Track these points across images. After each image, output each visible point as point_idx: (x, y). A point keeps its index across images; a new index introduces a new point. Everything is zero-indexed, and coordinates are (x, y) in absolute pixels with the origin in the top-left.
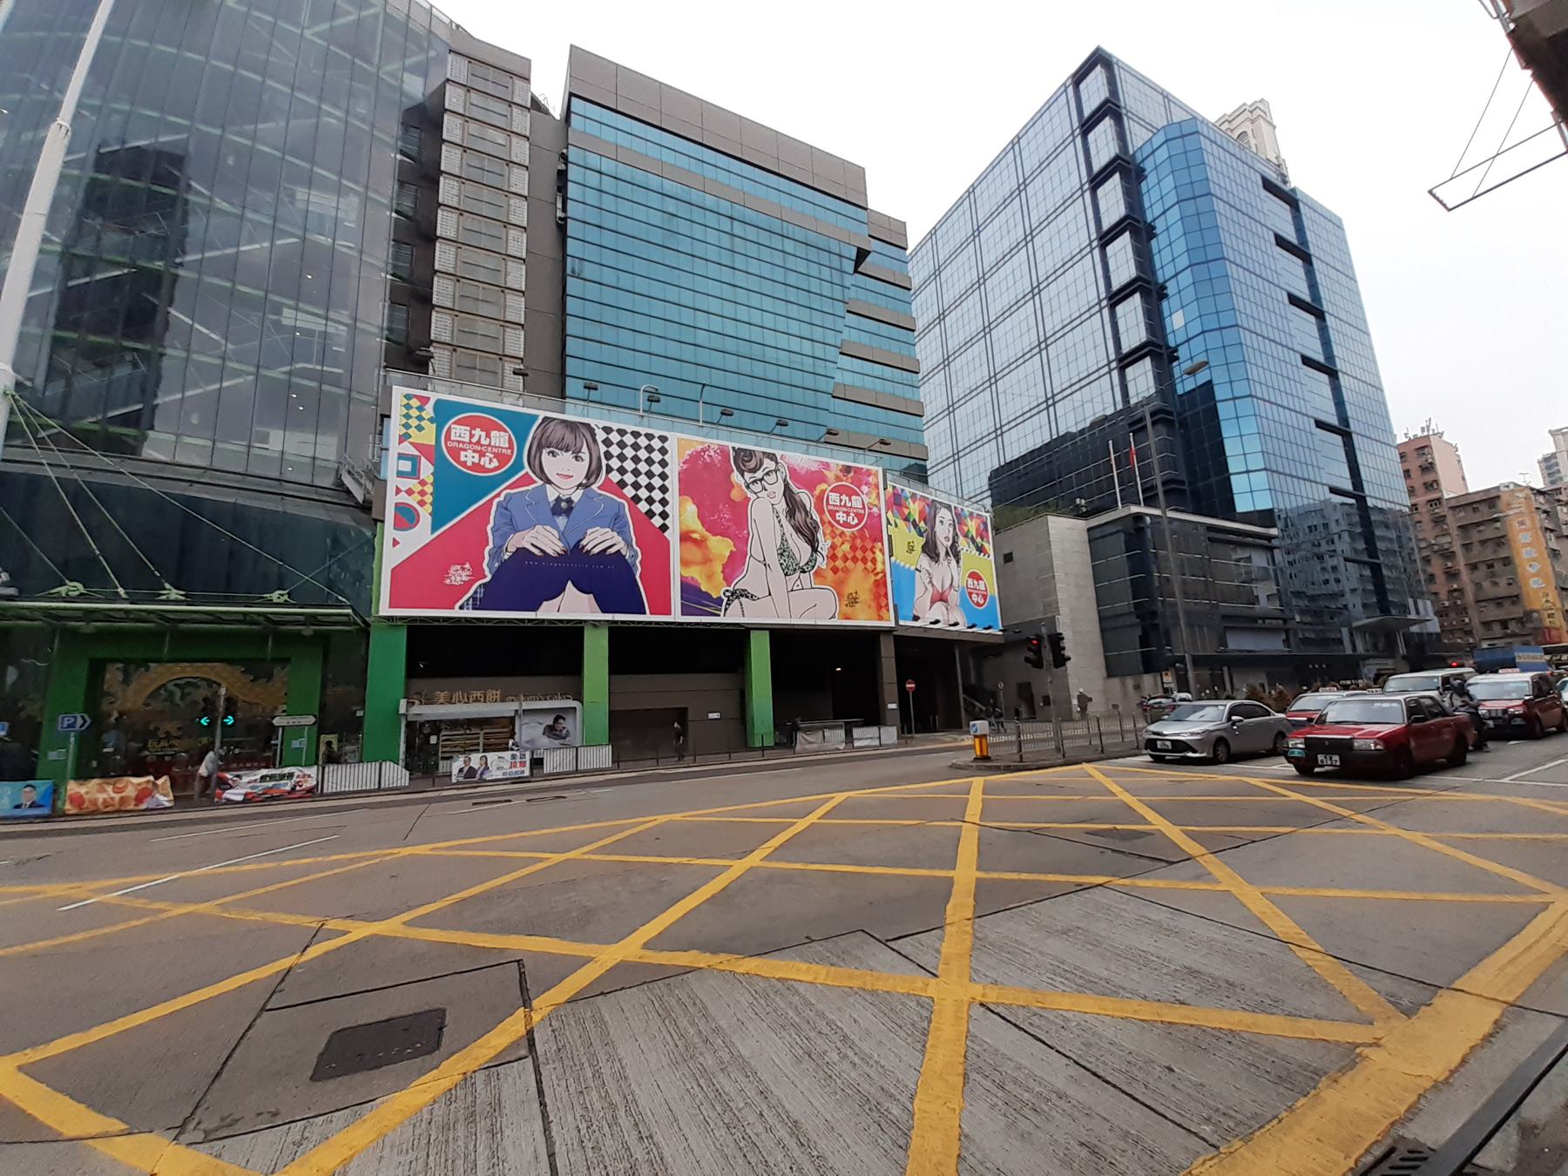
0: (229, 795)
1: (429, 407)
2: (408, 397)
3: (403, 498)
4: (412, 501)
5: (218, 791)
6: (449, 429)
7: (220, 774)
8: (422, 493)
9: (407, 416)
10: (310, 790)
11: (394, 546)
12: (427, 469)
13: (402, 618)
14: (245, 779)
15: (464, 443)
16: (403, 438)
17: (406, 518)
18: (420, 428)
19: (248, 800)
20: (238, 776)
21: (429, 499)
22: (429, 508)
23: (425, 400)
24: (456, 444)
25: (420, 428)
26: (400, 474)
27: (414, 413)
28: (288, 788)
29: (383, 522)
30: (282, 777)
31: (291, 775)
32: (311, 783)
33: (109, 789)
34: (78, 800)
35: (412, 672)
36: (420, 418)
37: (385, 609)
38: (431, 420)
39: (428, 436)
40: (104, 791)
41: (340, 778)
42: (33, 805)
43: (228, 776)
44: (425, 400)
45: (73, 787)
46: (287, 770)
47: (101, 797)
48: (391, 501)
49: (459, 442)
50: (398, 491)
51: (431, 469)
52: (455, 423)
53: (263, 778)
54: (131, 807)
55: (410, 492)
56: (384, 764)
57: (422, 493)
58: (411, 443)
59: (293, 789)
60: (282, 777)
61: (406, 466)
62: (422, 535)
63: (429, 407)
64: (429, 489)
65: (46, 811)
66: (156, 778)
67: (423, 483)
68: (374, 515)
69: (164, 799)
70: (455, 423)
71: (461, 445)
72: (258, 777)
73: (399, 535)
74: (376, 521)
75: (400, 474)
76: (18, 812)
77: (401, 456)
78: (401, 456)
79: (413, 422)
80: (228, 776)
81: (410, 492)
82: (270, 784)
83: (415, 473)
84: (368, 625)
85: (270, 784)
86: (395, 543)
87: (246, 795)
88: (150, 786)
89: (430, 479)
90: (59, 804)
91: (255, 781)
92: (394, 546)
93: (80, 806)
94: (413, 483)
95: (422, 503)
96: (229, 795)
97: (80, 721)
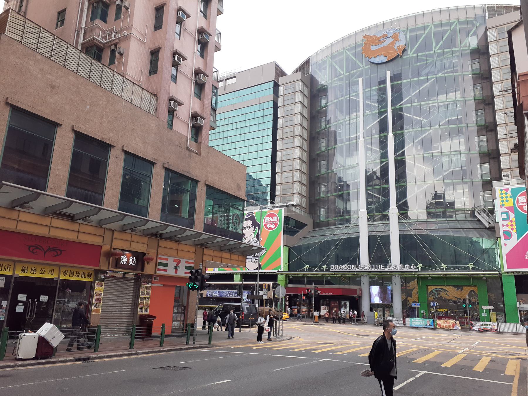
0: (474, 328)
1: (509, 192)
2: (501, 190)
3: (505, 228)
4: (509, 229)
5: (471, 327)
6: (518, 198)
7: (471, 322)
8: (512, 225)
9: (502, 198)
10: (496, 330)
11: (505, 246)
12: (512, 216)
13: (512, 272)
14: (478, 324)
15: (524, 203)
16: (502, 206)
17: (508, 236)
18: (507, 201)
19: (480, 331)
20: (475, 323)
21: (514, 227)
22: (515, 231)
23: (507, 190)
24: (521, 204)
25: (507, 201)
26: (503, 219)
27: (504, 196)
28: (490, 329)
29: (500, 238)
30: (487, 325)
31: (490, 325)
32: (496, 328)
33: (446, 323)
34: (439, 325)
35: (518, 291)
36: (507, 197)
37: (506, 270)
38: (511, 197)
39: (510, 204)
40: (445, 323)
41: (504, 327)
42: (430, 325)
43: (473, 322)
44: (507, 190)
45: (438, 321)
46: (489, 323)
47: (444, 325)
48: (502, 229)
49: (522, 203)
50: (503, 226)
51: (514, 215)
52: (519, 196)
53: (482, 324)
54: (451, 328)
55: (507, 225)
56: (517, 324)
57: (512, 225)
58: (505, 207)
59: (491, 329)
60: (487, 325)
61: (505, 216)
62: (514, 241)
63: (509, 192)
64: (514, 223)
65: (433, 327)
66: (456, 321)
67: (511, 221)
68: (497, 236)
69: (459, 327)
70: (519, 196)
71: (523, 204)
72: (481, 324)
73: (506, 242)
74: (497, 238)
75: (503, 219)
76: (426, 326)
77: (502, 213)
78: (502, 213)
79: (505, 199)
80: (473, 322)
81: (507, 225)
82: (485, 327)
83: (508, 218)
84: (501, 275)
85: (485, 327)
86: (505, 245)
87: (478, 329)
88: (455, 323)
89: (514, 220)
90: (435, 325)
91: (480, 325)
92: (505, 246)
93: (440, 326)
94: (508, 222)
95: (512, 229)
96: (474, 328)
97: (436, 304)
